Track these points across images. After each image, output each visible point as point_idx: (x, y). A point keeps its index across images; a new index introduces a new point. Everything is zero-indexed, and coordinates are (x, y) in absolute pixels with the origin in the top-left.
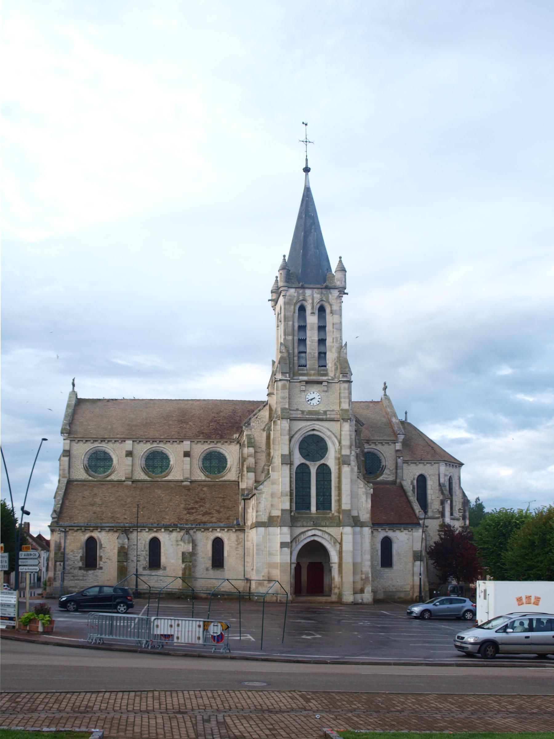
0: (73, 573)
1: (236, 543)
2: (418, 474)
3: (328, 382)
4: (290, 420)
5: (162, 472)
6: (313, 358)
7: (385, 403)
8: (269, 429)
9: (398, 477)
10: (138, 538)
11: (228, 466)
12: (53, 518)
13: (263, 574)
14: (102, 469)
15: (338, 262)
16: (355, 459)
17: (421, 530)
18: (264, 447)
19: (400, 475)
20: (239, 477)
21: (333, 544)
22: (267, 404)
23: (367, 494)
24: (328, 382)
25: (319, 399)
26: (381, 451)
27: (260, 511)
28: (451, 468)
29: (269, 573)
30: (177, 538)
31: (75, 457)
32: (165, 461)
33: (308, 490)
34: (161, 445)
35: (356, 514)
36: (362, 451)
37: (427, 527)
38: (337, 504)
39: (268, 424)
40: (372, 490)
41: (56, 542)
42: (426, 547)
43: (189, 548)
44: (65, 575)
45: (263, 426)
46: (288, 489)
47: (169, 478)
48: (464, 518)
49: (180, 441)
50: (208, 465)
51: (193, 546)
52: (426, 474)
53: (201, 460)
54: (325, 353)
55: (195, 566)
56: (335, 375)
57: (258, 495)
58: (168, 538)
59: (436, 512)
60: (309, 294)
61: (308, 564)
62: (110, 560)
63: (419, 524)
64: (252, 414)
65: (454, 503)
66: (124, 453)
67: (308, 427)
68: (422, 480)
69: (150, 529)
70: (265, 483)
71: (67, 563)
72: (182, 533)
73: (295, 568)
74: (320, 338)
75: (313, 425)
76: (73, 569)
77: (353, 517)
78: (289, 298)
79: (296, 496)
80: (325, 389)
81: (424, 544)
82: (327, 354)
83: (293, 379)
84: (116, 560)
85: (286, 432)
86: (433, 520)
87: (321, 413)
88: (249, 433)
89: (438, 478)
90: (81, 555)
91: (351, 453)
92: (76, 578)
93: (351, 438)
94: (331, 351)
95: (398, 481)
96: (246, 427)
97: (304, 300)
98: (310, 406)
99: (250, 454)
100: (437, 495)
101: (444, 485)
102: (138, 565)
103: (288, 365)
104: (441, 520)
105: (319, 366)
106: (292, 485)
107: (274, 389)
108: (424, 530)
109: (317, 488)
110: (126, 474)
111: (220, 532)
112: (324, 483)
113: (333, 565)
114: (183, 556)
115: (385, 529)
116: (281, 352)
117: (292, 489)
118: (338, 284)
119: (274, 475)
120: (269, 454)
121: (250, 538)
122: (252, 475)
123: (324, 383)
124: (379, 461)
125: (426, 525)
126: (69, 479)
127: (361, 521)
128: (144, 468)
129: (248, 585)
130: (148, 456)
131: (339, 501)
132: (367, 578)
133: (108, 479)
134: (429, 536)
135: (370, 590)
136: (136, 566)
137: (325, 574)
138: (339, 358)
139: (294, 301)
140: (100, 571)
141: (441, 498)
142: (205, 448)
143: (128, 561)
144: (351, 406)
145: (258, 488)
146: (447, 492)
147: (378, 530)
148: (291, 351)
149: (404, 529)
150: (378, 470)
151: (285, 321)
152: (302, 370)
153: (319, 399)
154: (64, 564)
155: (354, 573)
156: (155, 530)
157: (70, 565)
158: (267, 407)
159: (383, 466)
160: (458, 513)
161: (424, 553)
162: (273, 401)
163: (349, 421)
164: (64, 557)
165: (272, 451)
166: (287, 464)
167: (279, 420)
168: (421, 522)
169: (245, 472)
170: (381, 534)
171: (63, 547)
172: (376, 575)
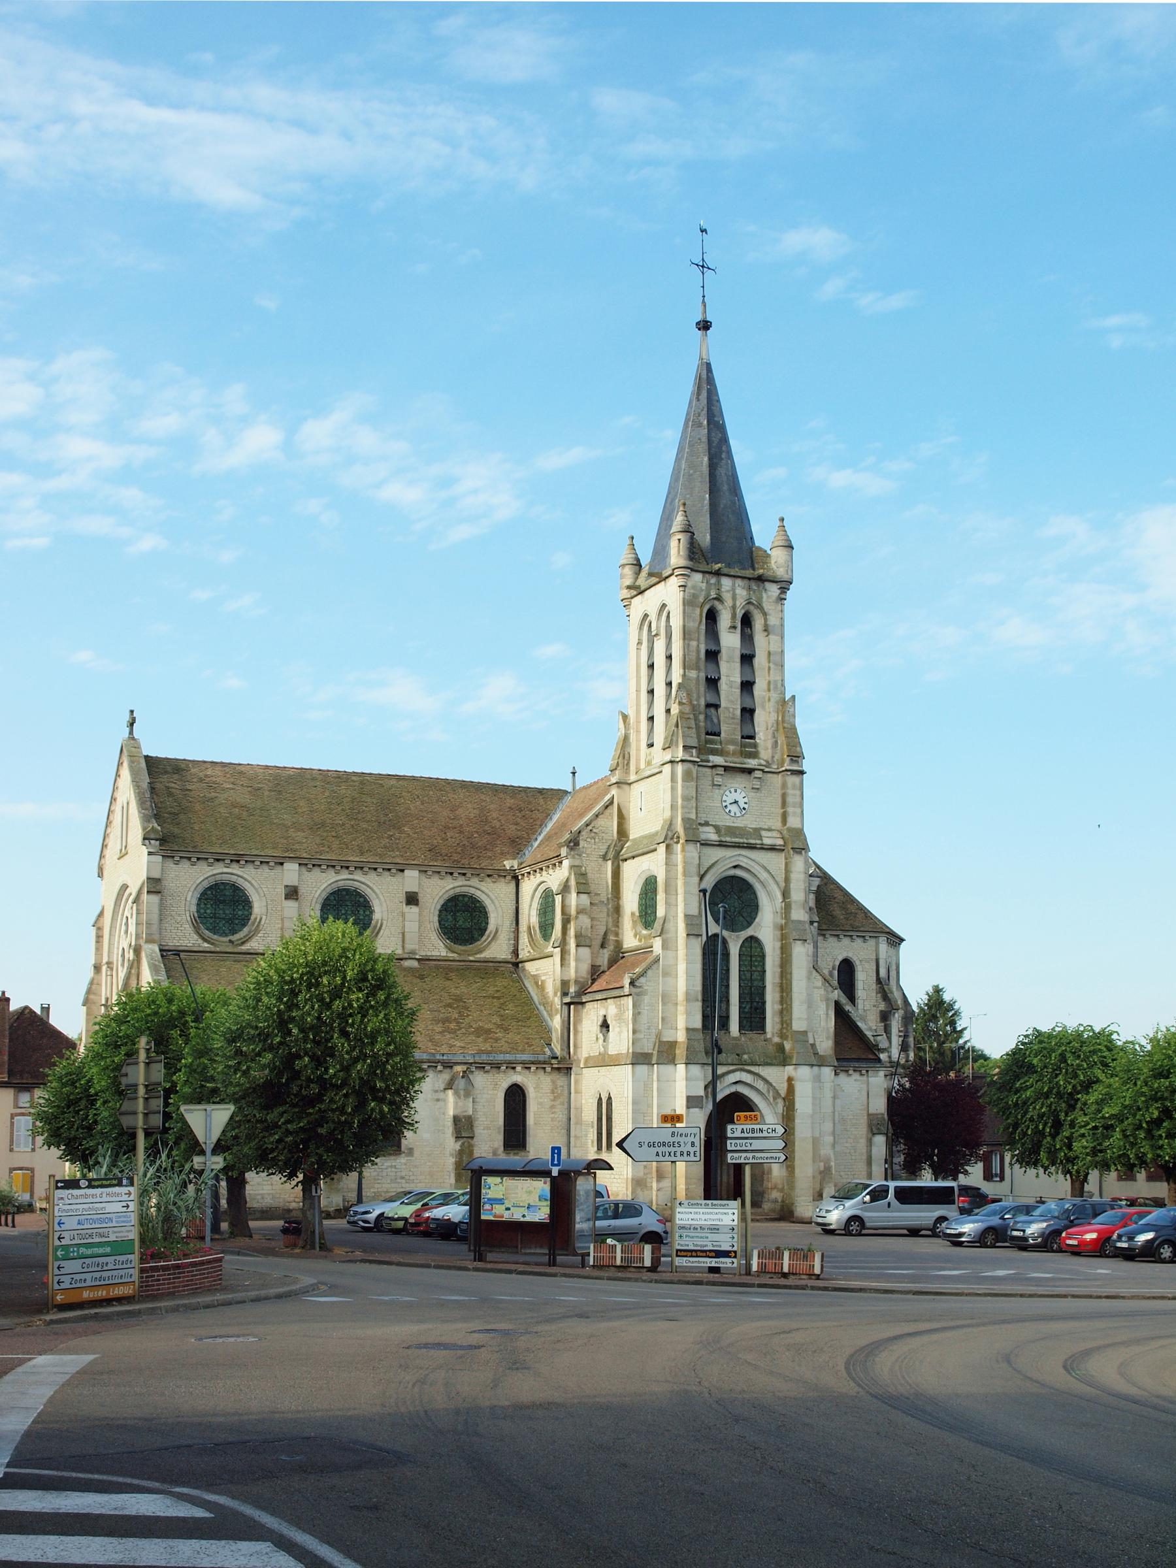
2: (840, 958)
75: (737, 858)
89: (875, 968)
94: (763, 708)
100: (873, 1002)
139: (701, 600)
141: (882, 1006)
152: (712, 742)
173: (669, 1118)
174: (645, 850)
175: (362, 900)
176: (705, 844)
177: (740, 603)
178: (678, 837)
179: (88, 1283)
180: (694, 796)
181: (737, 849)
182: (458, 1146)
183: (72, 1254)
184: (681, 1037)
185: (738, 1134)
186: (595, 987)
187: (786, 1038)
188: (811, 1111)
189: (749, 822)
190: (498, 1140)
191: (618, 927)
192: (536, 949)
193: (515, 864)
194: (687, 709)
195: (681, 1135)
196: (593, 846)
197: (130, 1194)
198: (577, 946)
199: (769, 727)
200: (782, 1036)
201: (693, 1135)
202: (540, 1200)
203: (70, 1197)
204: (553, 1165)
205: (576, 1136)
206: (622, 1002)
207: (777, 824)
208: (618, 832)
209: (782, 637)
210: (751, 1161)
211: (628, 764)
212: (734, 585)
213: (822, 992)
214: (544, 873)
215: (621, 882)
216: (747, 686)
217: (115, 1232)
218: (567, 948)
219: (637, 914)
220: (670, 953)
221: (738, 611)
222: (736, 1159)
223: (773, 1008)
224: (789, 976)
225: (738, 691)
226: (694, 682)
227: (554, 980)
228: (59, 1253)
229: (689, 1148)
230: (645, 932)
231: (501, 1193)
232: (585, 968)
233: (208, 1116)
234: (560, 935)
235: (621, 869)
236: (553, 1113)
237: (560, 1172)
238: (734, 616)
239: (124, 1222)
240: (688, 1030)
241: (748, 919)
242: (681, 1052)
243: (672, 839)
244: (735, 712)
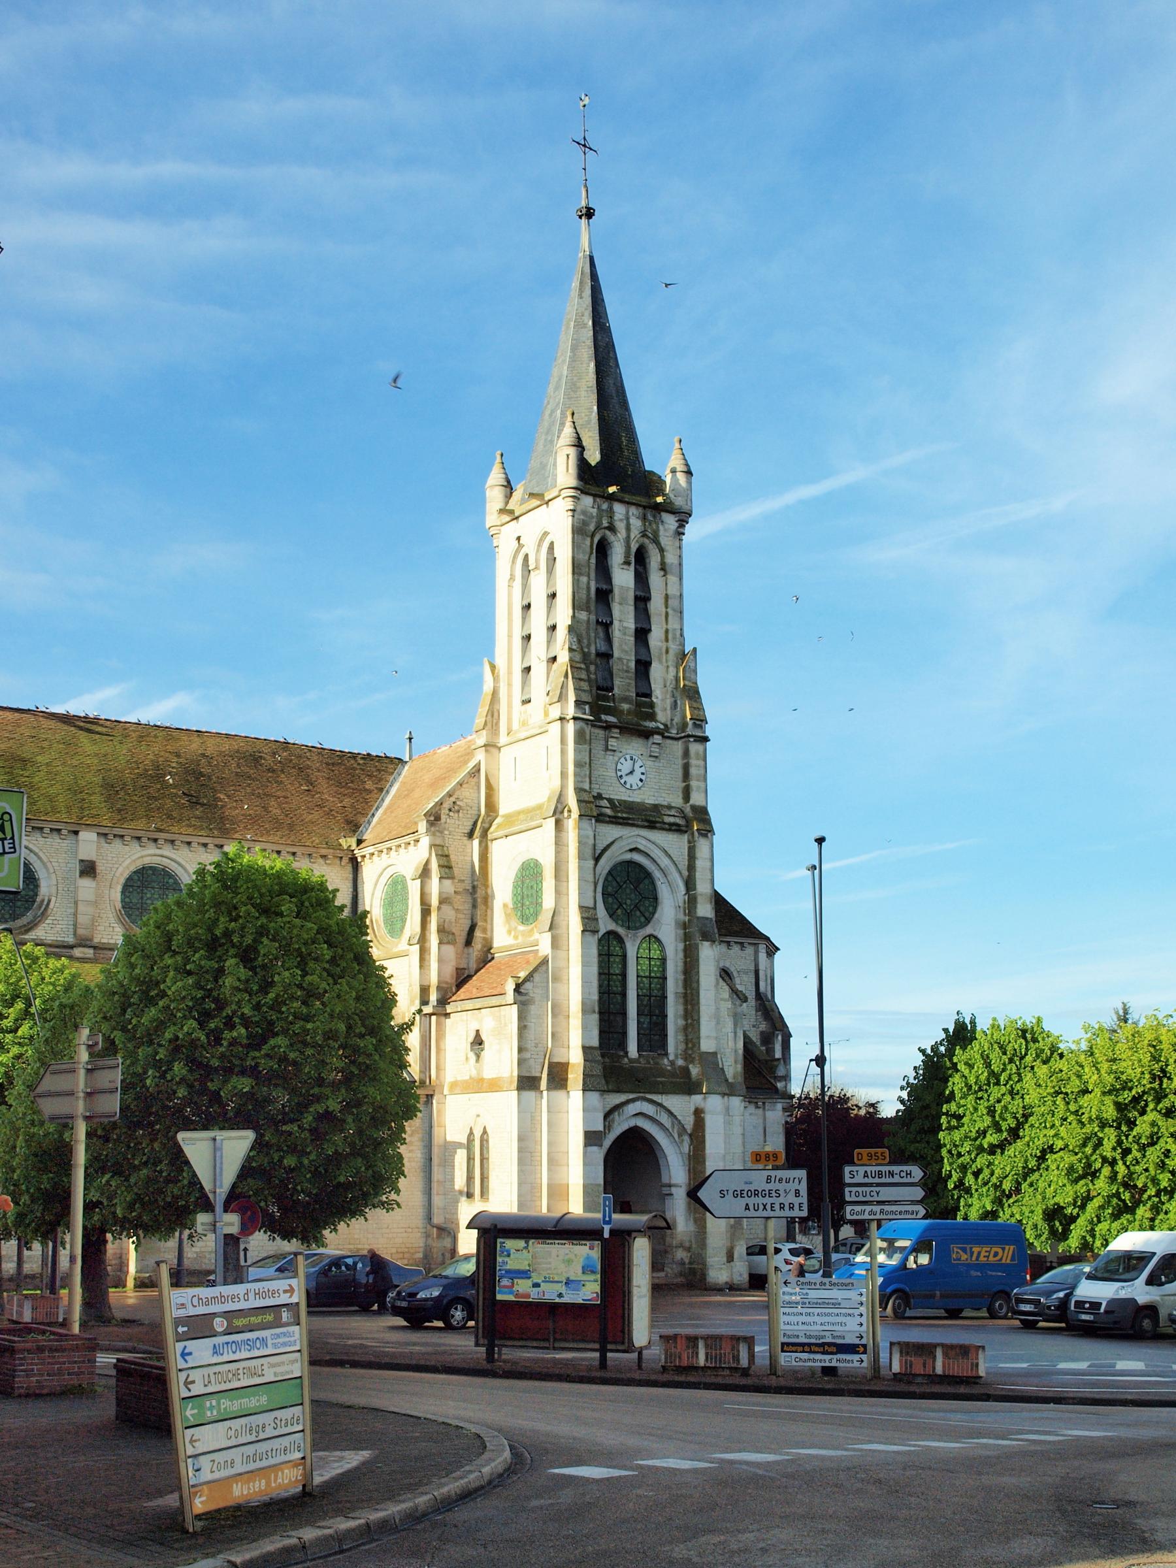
4: (597, 821)
6: (627, 671)
25: (643, 774)
56: (672, 720)
82: (654, 665)
97: (612, 528)
98: (623, 790)
105: (637, 695)
118: (679, 502)
153: (643, 774)
173: (763, 1157)
174: (523, 827)
175: (171, 881)
178: (570, 811)
179: (239, 1468)
180: (588, 761)
181: (634, 828)
183: (209, 1414)
184: (575, 1058)
185: (859, 1179)
186: (462, 993)
187: (692, 1062)
188: (722, 1152)
189: (647, 797)
191: (486, 921)
192: (380, 947)
193: (353, 842)
195: (780, 1180)
196: (457, 822)
197: (291, 1290)
198: (440, 943)
199: (668, 684)
200: (688, 1058)
201: (797, 1180)
202: (583, 1273)
203: (195, 1301)
204: (606, 1223)
206: (503, 1013)
207: (677, 800)
208: (487, 806)
210: (878, 1217)
211: (497, 723)
213: (729, 1005)
214: (393, 853)
215: (489, 866)
217: (273, 1366)
218: (427, 945)
219: (511, 906)
220: (561, 954)
222: (858, 1213)
223: (676, 1024)
224: (694, 985)
227: (410, 986)
228: (188, 1413)
229: (791, 1198)
230: (521, 928)
231: (527, 1263)
232: (449, 970)
233: (216, 1148)
234: (418, 929)
235: (490, 851)
237: (612, 1231)
239: (284, 1344)
240: (586, 1049)
241: (647, 914)
242: (575, 1077)
243: (562, 812)
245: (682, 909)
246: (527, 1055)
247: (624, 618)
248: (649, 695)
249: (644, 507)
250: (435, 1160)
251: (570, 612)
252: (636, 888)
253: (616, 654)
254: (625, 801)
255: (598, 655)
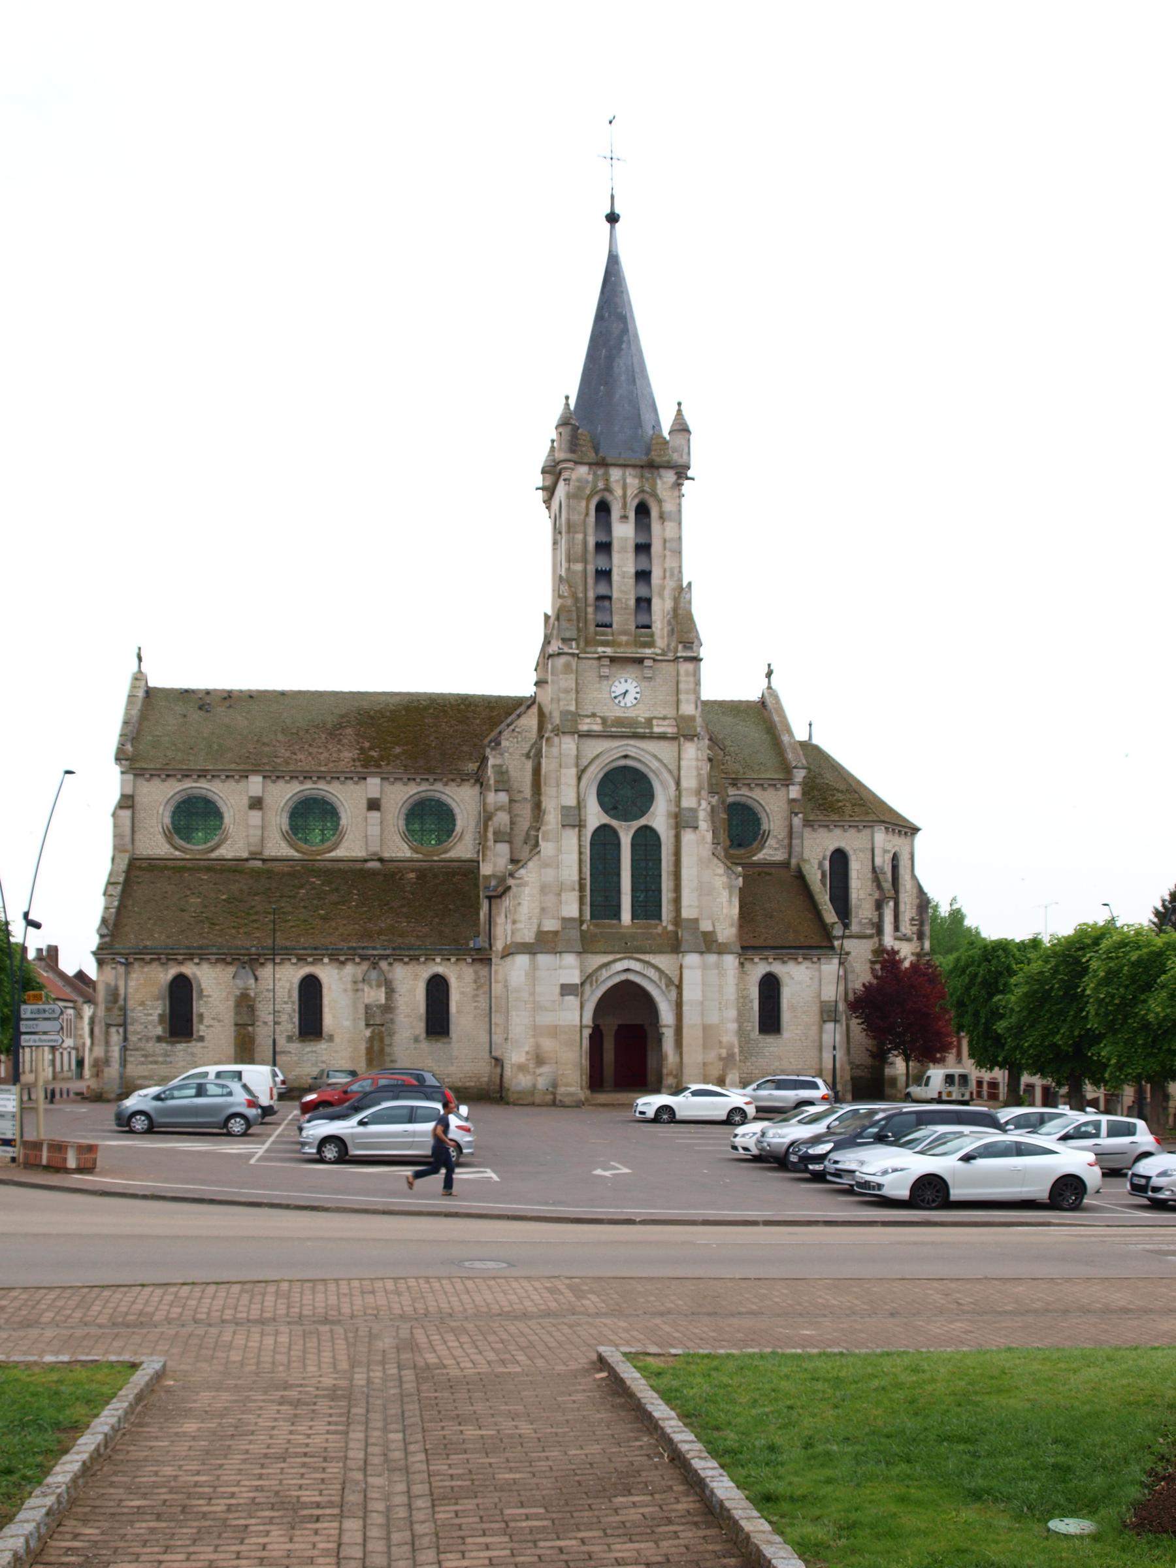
0: (143, 1050)
1: (474, 986)
2: (832, 848)
3: (654, 660)
4: (580, 736)
5: (322, 841)
7: (770, 701)
8: (539, 754)
9: (794, 854)
10: (277, 976)
11: (458, 829)
12: (102, 936)
13: (527, 1049)
14: (200, 834)
15: (675, 413)
16: (709, 818)
17: (836, 961)
18: (528, 792)
19: (796, 849)
20: (479, 852)
21: (664, 987)
22: (534, 703)
23: (730, 888)
24: (654, 660)
26: (761, 802)
27: (520, 922)
28: (896, 836)
29: (537, 1046)
30: (354, 976)
31: (145, 809)
32: (329, 819)
33: (615, 879)
34: (322, 785)
35: (710, 929)
36: (723, 802)
37: (848, 954)
38: (671, 908)
39: (535, 743)
40: (741, 879)
41: (108, 985)
42: (846, 994)
43: (380, 996)
44: (128, 1052)
45: (526, 747)
46: (576, 877)
47: (339, 853)
48: (921, 936)
49: (359, 778)
50: (417, 827)
51: (386, 993)
52: (848, 849)
53: (402, 817)
54: (649, 601)
55: (391, 1034)
56: (668, 645)
57: (514, 889)
58: (337, 977)
59: (867, 923)
60: (617, 478)
61: (615, 1027)
62: (219, 1021)
63: (832, 948)
64: (503, 726)
65: (902, 907)
66: (245, 802)
67: (614, 752)
68: (840, 859)
69: (301, 959)
70: (530, 864)
71: (130, 1028)
72: (365, 966)
73: (591, 1036)
74: (640, 568)
76: (144, 1042)
77: (703, 932)
78: (577, 484)
79: (591, 890)
80: (648, 673)
81: (841, 988)
83: (586, 653)
84: (232, 1022)
85: (572, 761)
86: (861, 940)
87: (641, 723)
88: (498, 762)
89: (870, 857)
90: (160, 1012)
91: (700, 805)
92: (150, 1059)
93: (699, 775)
95: (794, 861)
96: (493, 749)
99: (499, 804)
100: (869, 891)
101: (882, 869)
102: (278, 1030)
103: (575, 623)
104: (876, 939)
105: (637, 627)
106: (584, 869)
107: (547, 672)
108: (842, 961)
109: (633, 876)
110: (249, 844)
111: (440, 964)
112: (647, 864)
113: (664, 1030)
114: (366, 1013)
115: (767, 959)
116: (560, 596)
117: (583, 876)
119: (546, 848)
120: (538, 807)
121: (500, 977)
122: (503, 849)
123: (646, 661)
124: (757, 822)
125: (847, 949)
126: (134, 854)
127: (720, 941)
128: (287, 832)
129: (498, 1070)
130: (296, 808)
131: (677, 901)
132: (731, 1056)
133: (214, 855)
134: (853, 972)
135: (738, 1080)
136: (271, 1034)
137: (649, 1048)
138: (675, 610)
140: (200, 1044)
141: (877, 895)
142: (411, 793)
143: (257, 1024)
144: (700, 709)
145: (516, 875)
146: (887, 885)
147: (752, 959)
148: (581, 595)
149: (804, 959)
150: (755, 839)
151: (568, 532)
154: (125, 1032)
155: (705, 1046)
156: (310, 959)
157: (138, 1033)
158: (535, 709)
159: (765, 831)
160: (909, 927)
161: (842, 1006)
162: (545, 698)
163: (696, 739)
164: (125, 1015)
165: (543, 798)
166: (574, 826)
167: (557, 735)
168: (836, 943)
169: (491, 843)
170: (759, 969)
171: (122, 996)
172: (747, 1050)
176: (589, 735)
177: (630, 492)
182: (368, 1033)
190: (420, 1027)
194: (569, 602)
205: (495, 1024)
209: (680, 524)
212: (624, 474)
216: (643, 576)
221: (629, 500)
225: (631, 581)
226: (580, 575)
236: (476, 1002)
238: (624, 506)
244: (629, 602)
245: (673, 803)
246: (519, 926)
247: (623, 564)
248: (649, 627)
249: (642, 467)
250: (493, 1010)
251: (567, 565)
252: (632, 788)
253: (615, 595)
254: (619, 718)
255: (599, 598)
